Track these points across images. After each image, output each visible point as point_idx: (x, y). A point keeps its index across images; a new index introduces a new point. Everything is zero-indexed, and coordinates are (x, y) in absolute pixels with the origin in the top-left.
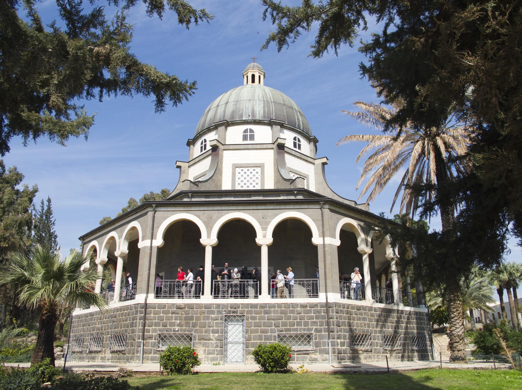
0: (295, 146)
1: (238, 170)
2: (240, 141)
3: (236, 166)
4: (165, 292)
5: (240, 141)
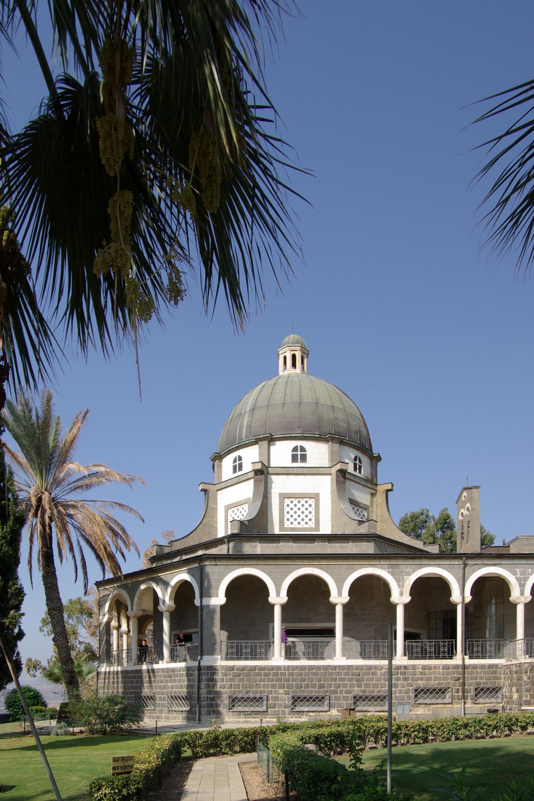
0: (355, 469)
1: (287, 501)
2: (288, 462)
3: (283, 497)
4: (246, 653)
5: (288, 462)
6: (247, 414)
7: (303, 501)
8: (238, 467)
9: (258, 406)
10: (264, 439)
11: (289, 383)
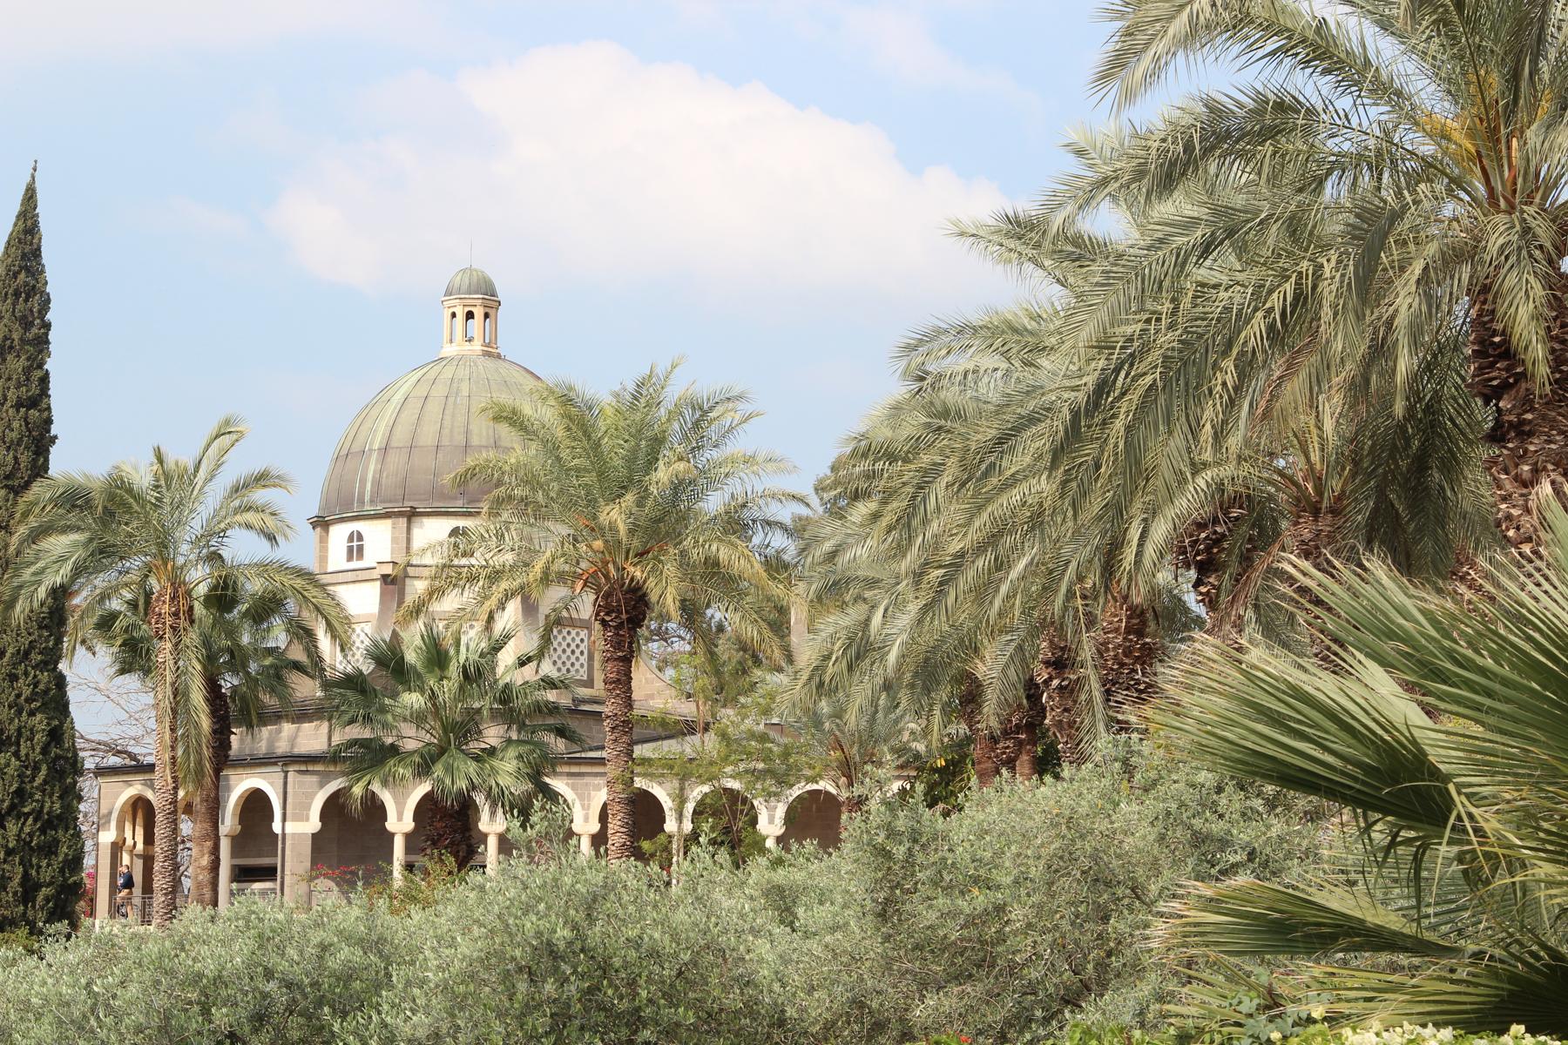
6: (375, 456)
8: (356, 549)
9: (394, 443)
10: (400, 514)
11: (451, 400)
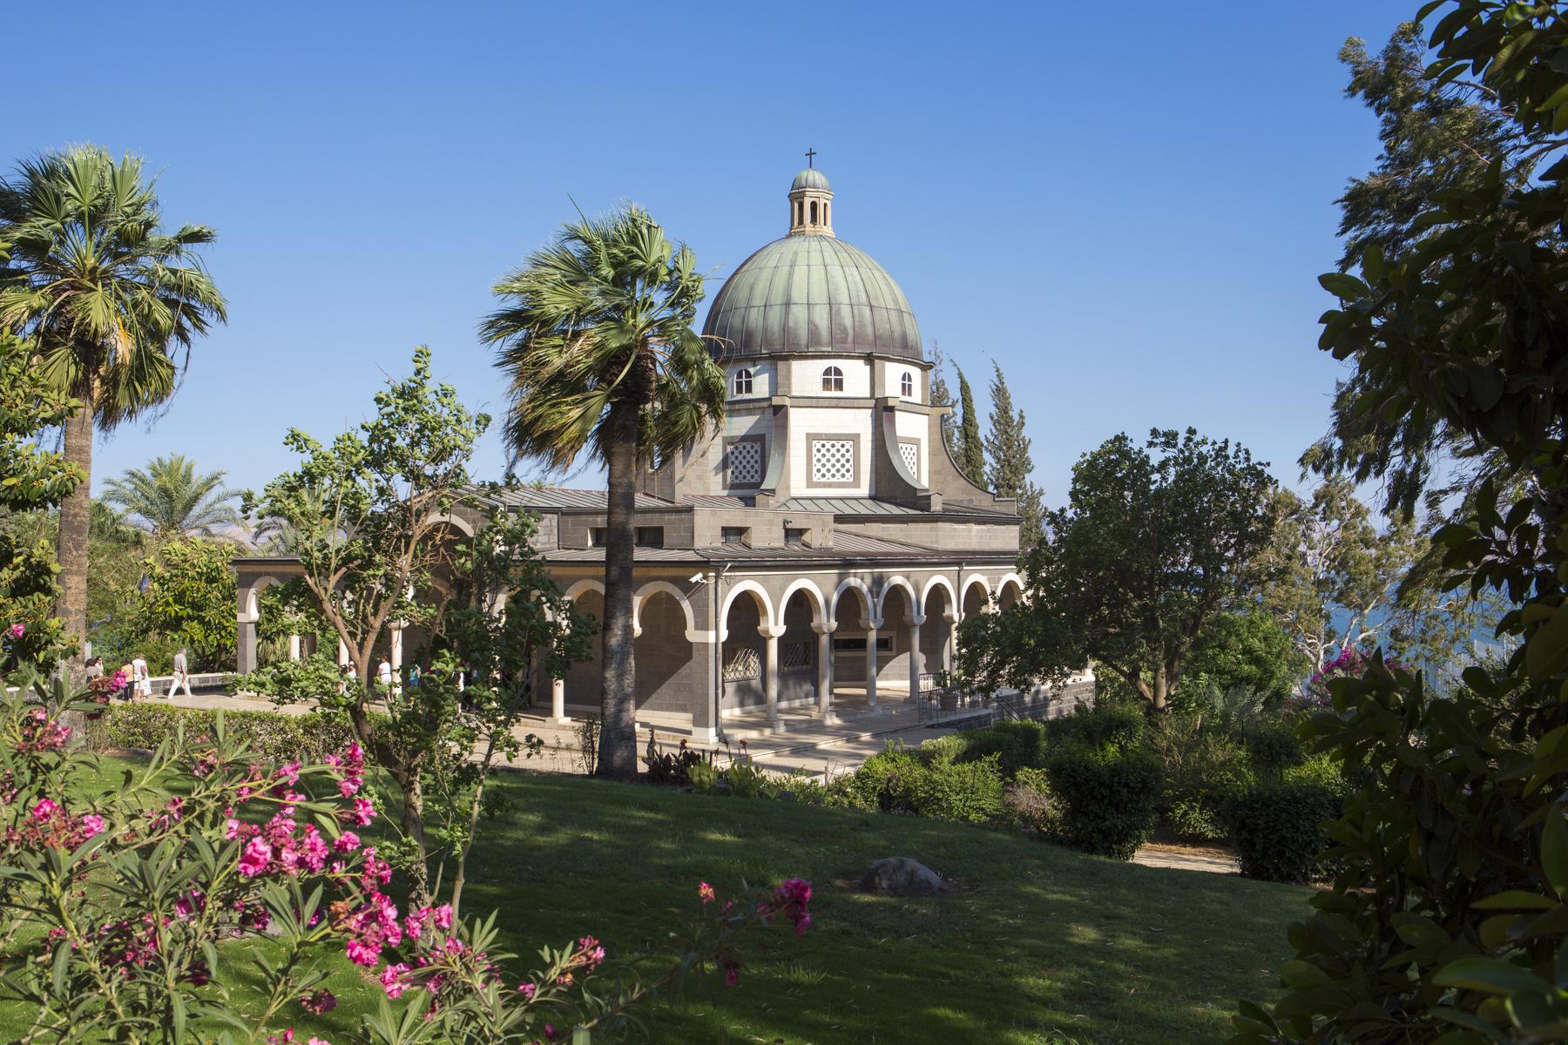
1: (817, 444)
2: (817, 390)
3: (811, 437)
5: (817, 390)
7: (838, 445)
